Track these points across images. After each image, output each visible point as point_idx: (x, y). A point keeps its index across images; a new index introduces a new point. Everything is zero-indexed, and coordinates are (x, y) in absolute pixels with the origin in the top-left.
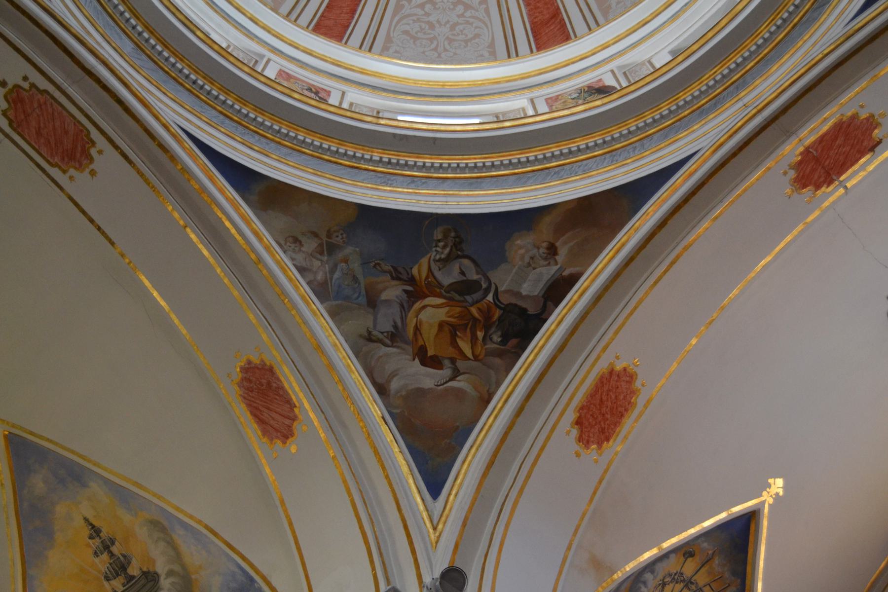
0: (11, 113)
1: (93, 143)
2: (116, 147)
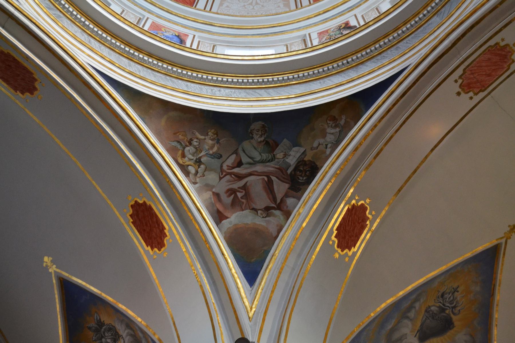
0: (476, 91)
1: (497, 44)
2: (500, 30)
